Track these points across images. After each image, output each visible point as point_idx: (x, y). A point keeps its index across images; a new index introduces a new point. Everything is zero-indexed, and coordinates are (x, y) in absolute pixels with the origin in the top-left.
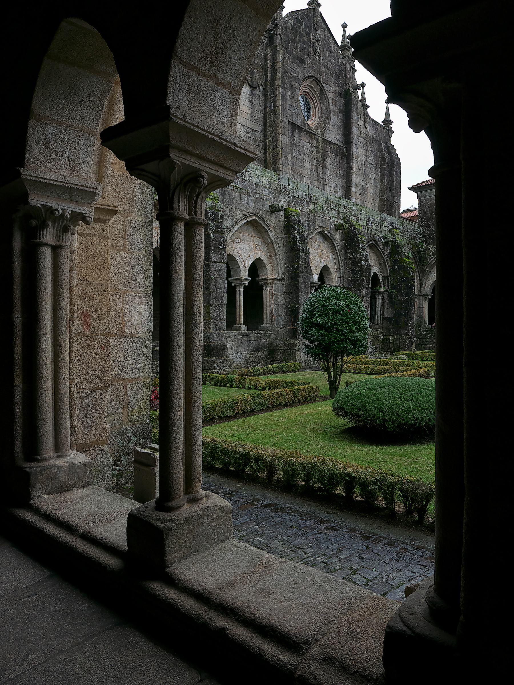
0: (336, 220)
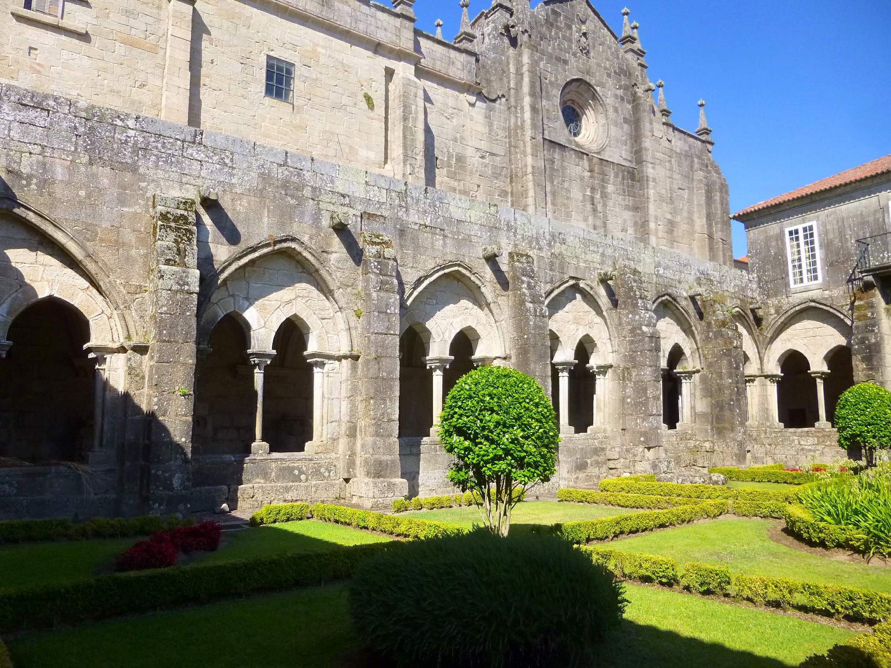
0: (599, 267)
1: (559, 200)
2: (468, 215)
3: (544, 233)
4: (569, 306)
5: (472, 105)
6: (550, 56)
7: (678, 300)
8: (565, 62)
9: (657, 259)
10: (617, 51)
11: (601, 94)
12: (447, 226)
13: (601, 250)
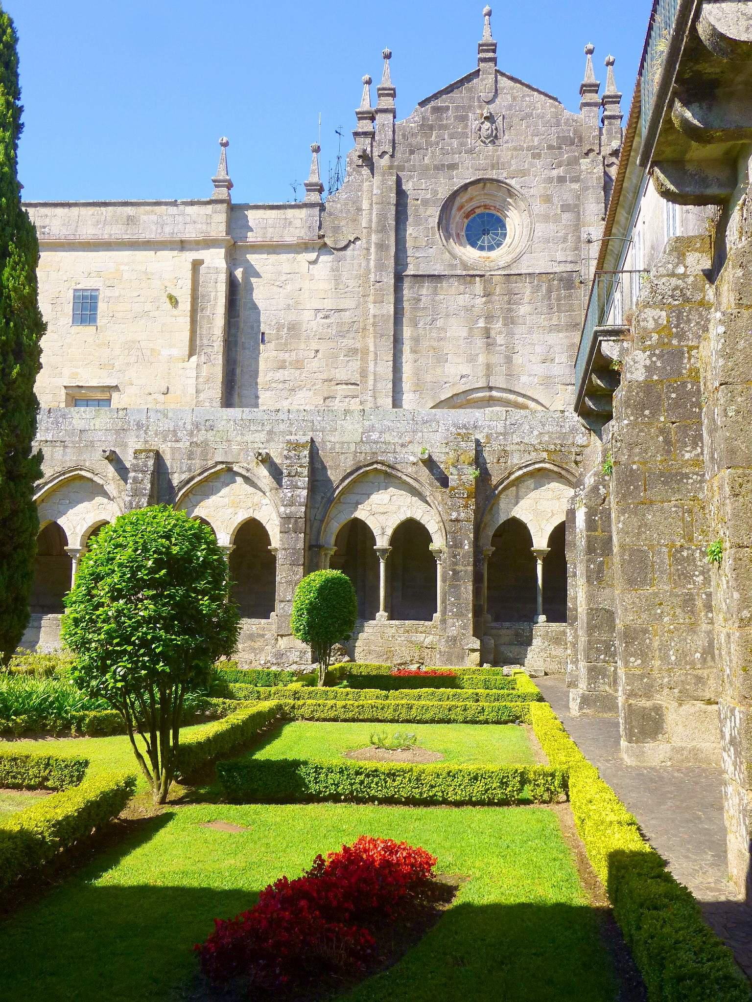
1: (425, 344)
2: (92, 424)
3: (185, 423)
4: (225, 491)
5: (315, 262)
6: (426, 168)
7: (398, 467)
8: (453, 167)
9: (367, 423)
10: (556, 116)
11: (518, 187)
12: (69, 437)
13: (268, 428)
